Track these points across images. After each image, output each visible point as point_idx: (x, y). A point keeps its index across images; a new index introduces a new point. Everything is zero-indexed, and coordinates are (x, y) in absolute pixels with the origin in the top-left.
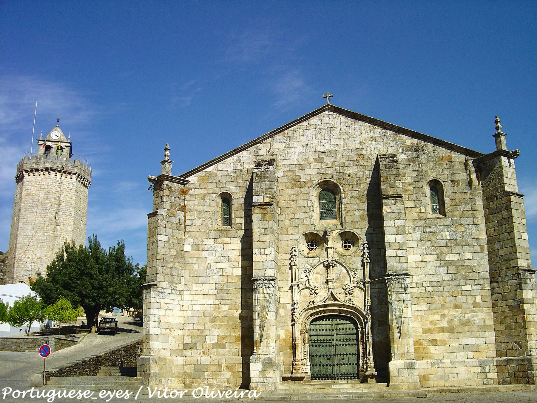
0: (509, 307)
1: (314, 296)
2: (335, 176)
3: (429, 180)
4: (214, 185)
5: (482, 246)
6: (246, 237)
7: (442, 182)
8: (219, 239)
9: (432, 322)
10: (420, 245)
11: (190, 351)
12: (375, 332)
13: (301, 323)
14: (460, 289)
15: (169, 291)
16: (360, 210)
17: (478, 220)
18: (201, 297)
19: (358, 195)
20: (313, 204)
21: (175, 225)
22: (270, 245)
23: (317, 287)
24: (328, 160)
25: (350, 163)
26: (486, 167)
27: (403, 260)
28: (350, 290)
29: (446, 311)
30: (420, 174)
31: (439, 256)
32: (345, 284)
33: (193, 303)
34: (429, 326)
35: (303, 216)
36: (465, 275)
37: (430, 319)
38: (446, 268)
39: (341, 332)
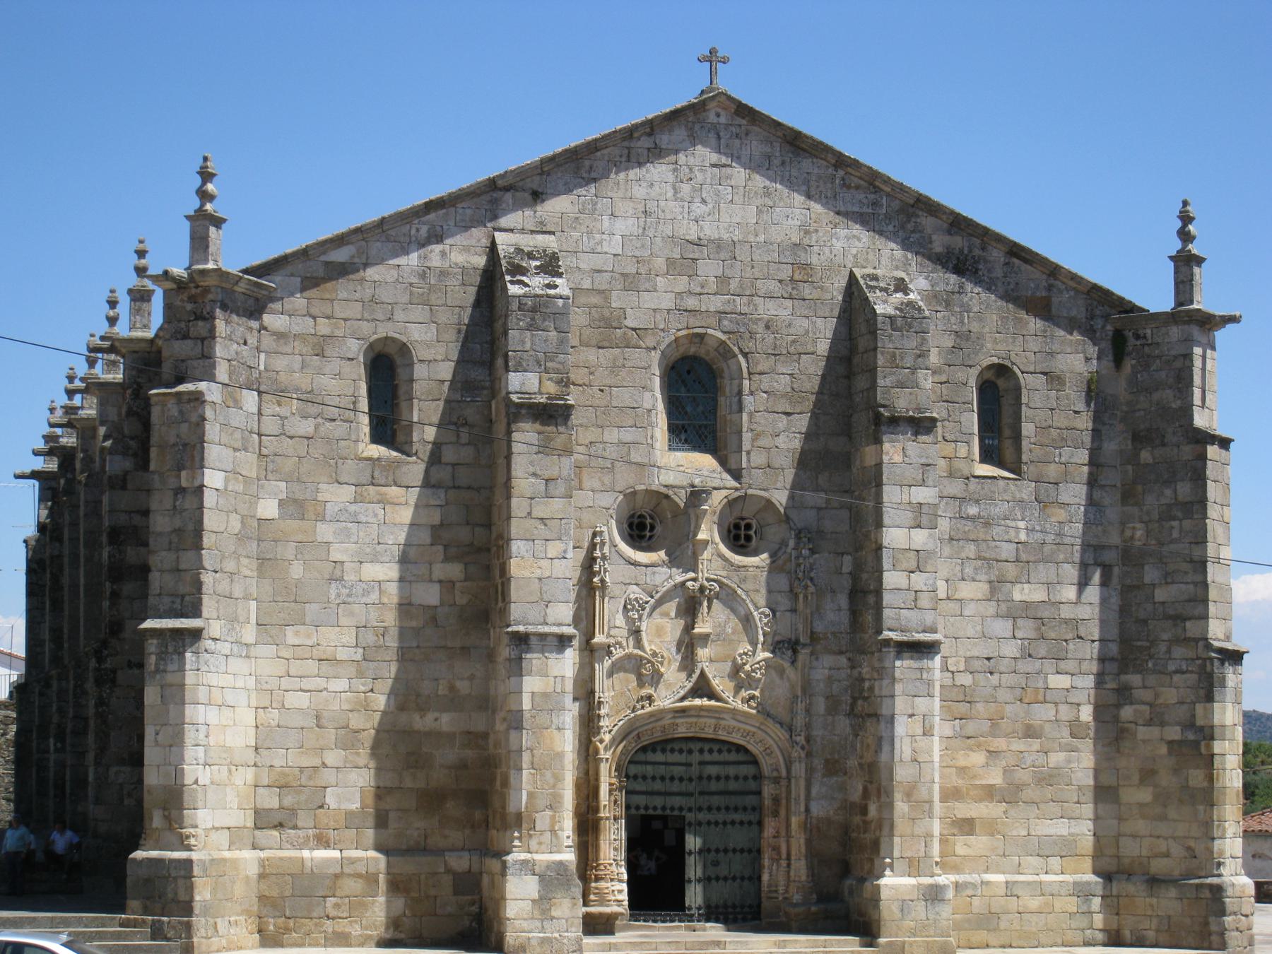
0: (1170, 743)
2: (726, 323)
3: (986, 363)
4: (355, 310)
6: (454, 487)
7: (1019, 374)
8: (371, 487)
9: (962, 770)
11: (275, 833)
12: (814, 791)
14: (1040, 684)
17: (1104, 494)
18: (312, 666)
19: (789, 390)
24: (709, 269)
25: (773, 286)
26: (1143, 345)
27: (924, 601)
29: (1000, 743)
30: (963, 341)
31: (996, 585)
33: (285, 683)
35: (628, 435)
37: (962, 762)
38: (1010, 622)
39: (714, 786)
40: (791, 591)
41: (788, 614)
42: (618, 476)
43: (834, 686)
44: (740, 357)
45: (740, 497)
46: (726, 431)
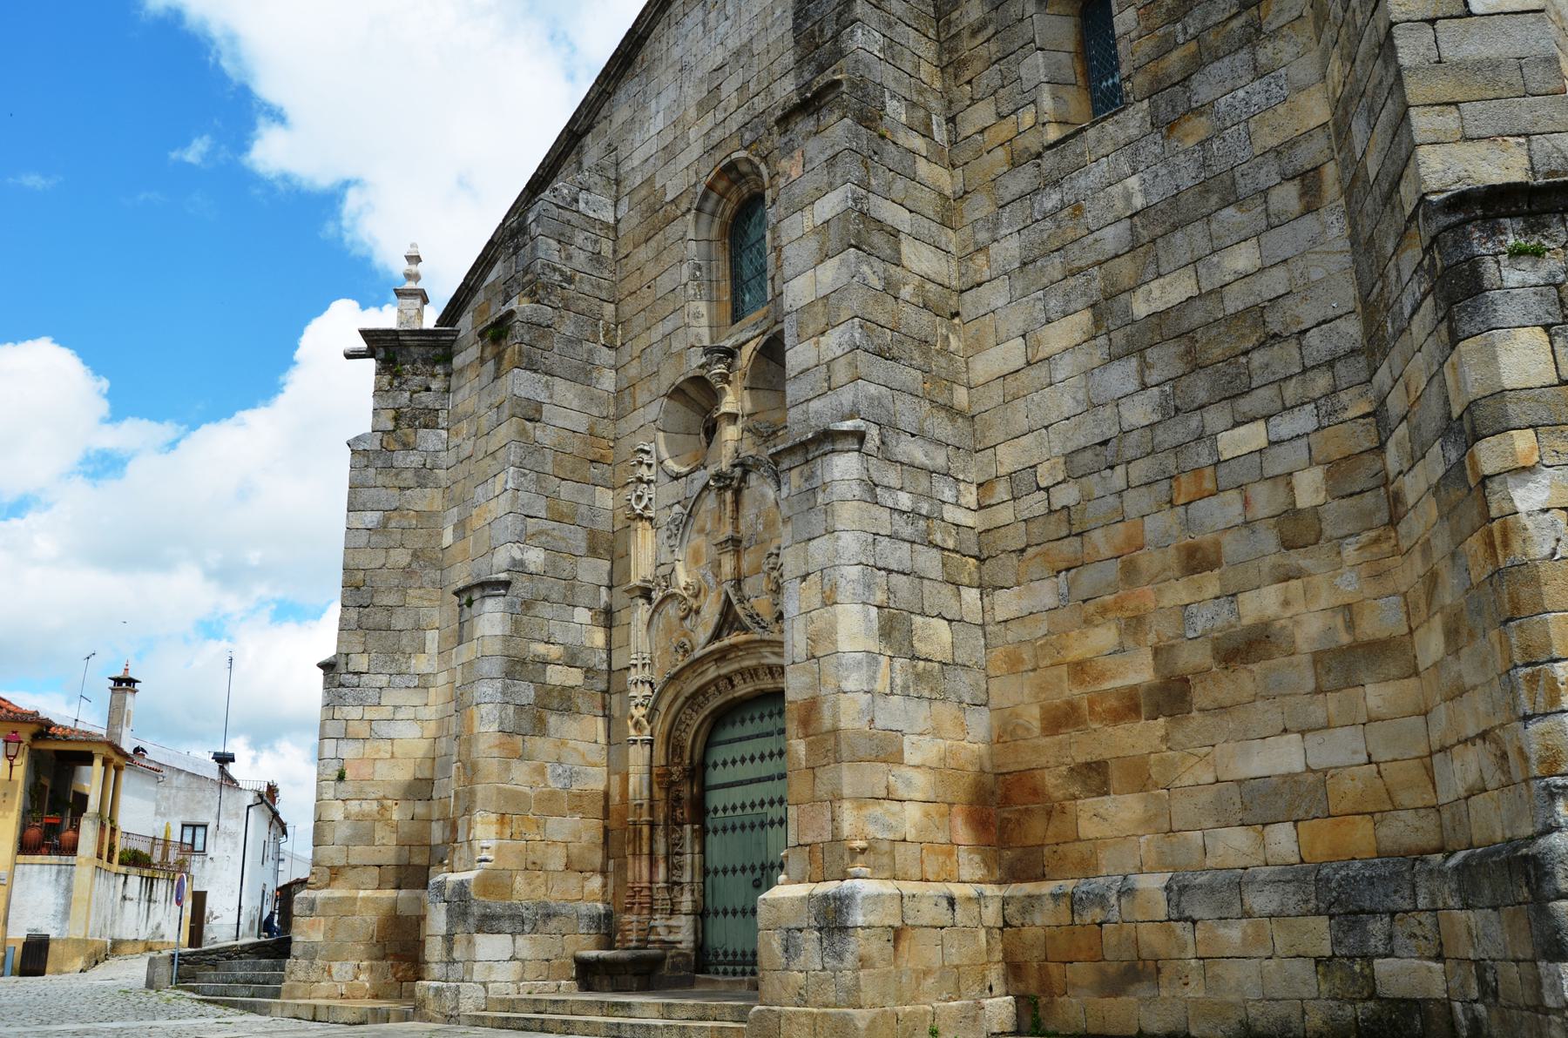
5: (1309, 181)
9: (1080, 669)
10: (1019, 285)
14: (1205, 460)
15: (383, 680)
21: (409, 475)
34: (1071, 691)
36: (1232, 370)
37: (1076, 653)
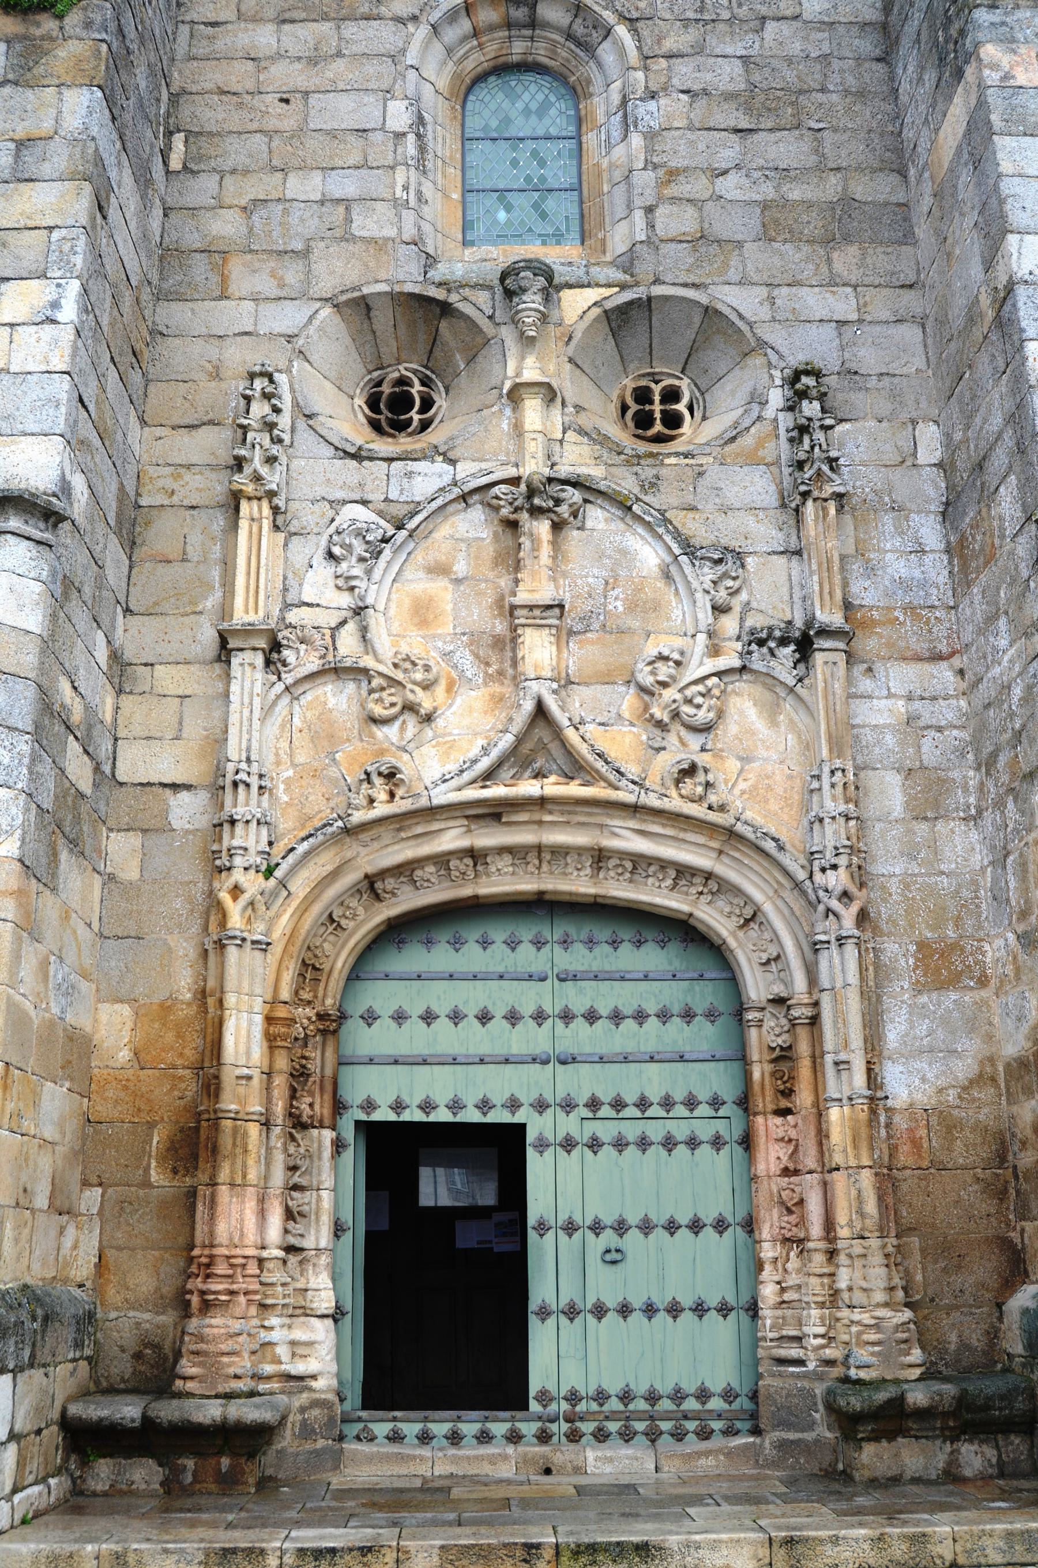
1: (394, 740)
12: (893, 1036)
13: (277, 950)
16: (756, 175)
20: (424, 125)
22: (53, 257)
23: (427, 668)
28: (689, 701)
32: (651, 650)
35: (344, 185)
40: (784, 505)
41: (782, 560)
42: (319, 268)
43: (927, 744)
44: (621, 31)
45: (631, 303)
46: (601, 194)
